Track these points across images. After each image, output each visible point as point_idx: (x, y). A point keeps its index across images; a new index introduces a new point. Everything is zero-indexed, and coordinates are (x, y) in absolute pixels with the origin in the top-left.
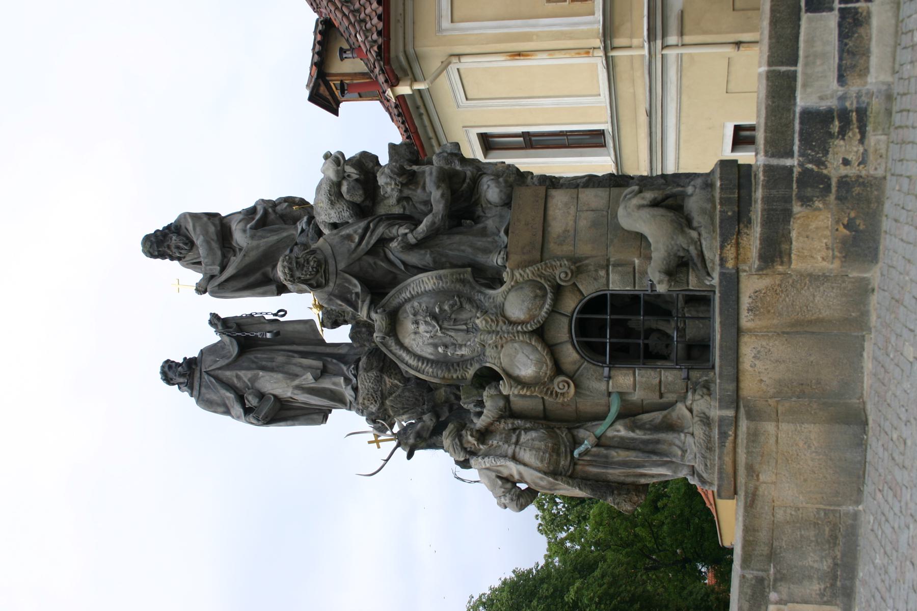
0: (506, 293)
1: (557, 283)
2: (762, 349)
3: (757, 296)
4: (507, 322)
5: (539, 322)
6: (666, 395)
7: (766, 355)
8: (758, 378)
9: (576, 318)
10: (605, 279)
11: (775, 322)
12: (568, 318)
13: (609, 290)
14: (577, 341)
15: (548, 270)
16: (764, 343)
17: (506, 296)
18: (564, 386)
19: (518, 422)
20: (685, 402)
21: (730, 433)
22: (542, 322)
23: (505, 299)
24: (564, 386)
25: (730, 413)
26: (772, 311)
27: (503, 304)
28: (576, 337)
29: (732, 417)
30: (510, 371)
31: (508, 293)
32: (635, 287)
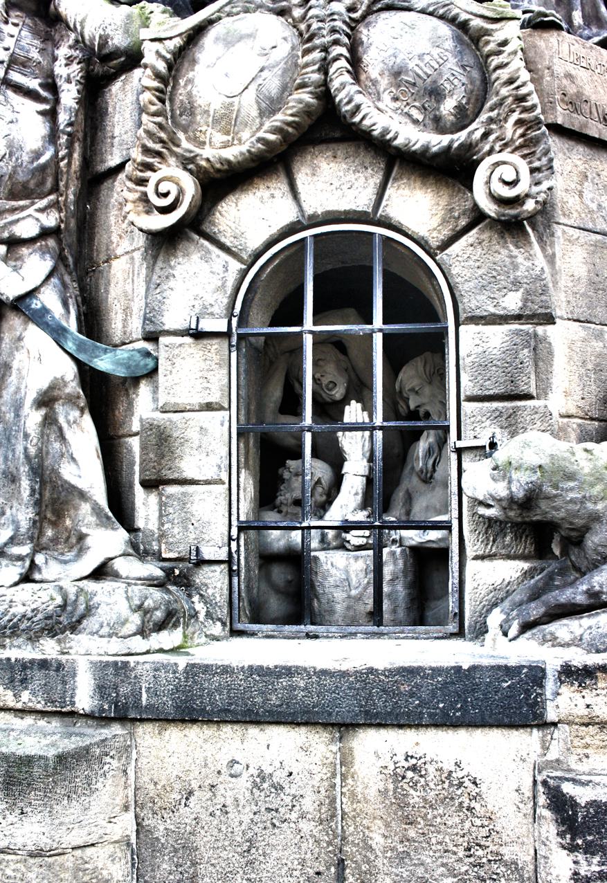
0: (441, 11)
1: (478, 162)
2: (288, 800)
3: (460, 785)
4: (354, 15)
5: (358, 108)
6: (153, 498)
7: (269, 810)
8: (195, 785)
9: (372, 234)
10: (492, 310)
11: (377, 840)
12: (370, 210)
13: (457, 325)
14: (303, 240)
15: (520, 131)
16: (309, 804)
17: (431, 14)
18: (166, 195)
19: (69, 96)
20: (125, 555)
21: (25, 696)
22: (357, 119)
23: (423, 11)
24: (166, 195)
25: (84, 699)
26: (412, 833)
27: (409, 9)
28: (315, 236)
29: (73, 703)
30: (209, 39)
31: (441, 17)
32: (471, 399)
